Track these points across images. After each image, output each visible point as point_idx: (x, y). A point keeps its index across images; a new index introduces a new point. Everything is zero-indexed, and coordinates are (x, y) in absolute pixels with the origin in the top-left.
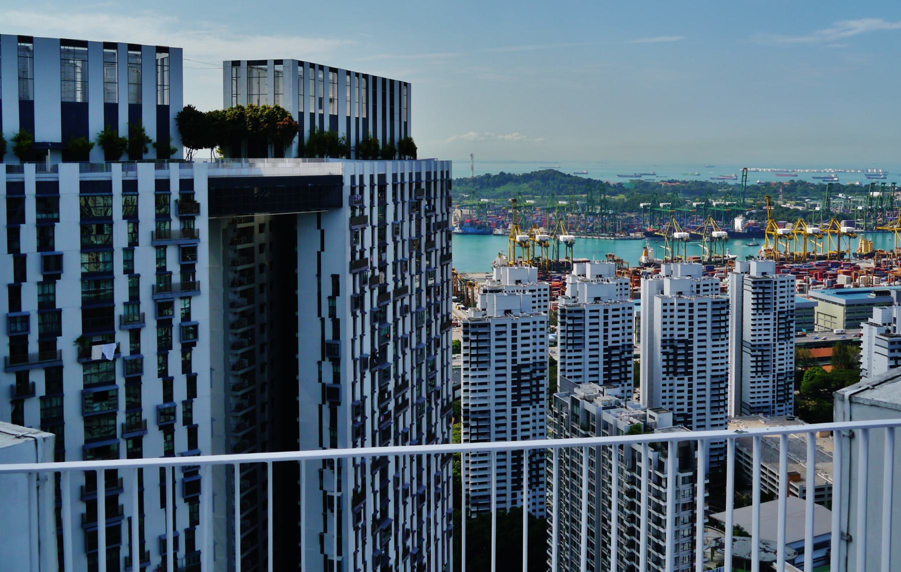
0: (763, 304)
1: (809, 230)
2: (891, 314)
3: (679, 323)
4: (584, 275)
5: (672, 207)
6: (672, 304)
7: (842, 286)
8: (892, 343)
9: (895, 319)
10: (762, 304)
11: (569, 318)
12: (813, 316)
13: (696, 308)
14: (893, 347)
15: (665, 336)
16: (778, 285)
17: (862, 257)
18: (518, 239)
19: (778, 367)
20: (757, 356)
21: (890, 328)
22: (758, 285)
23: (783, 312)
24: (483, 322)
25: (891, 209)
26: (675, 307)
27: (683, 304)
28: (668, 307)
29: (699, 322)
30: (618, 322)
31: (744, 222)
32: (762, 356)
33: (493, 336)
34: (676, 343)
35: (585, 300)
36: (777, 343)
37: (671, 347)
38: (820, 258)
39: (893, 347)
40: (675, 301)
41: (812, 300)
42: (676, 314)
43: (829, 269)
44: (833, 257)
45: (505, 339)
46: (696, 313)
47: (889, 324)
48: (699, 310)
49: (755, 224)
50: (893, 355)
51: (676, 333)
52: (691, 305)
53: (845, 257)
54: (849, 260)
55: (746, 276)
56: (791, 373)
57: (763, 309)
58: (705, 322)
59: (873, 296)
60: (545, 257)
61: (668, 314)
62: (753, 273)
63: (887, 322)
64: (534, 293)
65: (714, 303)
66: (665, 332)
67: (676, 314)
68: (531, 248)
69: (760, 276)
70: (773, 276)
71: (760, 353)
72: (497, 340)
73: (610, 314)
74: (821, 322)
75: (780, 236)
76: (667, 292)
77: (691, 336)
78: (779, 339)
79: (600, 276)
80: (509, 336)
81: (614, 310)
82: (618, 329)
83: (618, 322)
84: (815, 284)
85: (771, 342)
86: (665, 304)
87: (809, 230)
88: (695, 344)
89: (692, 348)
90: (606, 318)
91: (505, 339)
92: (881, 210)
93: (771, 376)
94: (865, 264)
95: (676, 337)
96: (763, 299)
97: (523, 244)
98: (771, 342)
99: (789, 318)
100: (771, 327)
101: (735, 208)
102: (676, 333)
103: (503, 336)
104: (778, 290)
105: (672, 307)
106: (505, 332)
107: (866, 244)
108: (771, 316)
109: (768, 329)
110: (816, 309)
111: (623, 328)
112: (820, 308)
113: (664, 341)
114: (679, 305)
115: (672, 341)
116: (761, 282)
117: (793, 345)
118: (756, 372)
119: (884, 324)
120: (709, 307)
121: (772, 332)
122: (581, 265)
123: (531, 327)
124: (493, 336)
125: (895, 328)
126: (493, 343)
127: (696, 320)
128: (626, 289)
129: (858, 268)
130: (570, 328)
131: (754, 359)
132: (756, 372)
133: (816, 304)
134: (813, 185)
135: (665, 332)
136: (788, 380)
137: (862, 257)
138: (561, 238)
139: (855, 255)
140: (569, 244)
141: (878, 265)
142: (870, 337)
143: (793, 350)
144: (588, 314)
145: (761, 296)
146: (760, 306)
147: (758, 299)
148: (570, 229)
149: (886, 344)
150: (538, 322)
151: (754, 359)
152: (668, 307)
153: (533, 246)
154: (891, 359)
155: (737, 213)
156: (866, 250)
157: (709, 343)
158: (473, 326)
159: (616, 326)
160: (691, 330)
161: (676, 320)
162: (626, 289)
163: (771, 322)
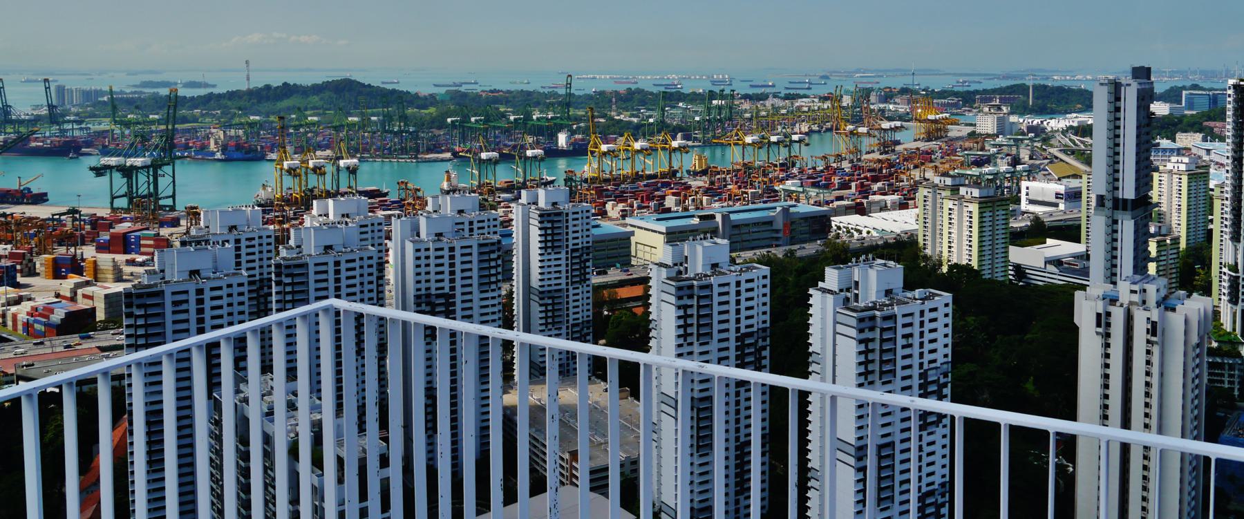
0: (553, 241)
1: (637, 145)
2: (683, 251)
3: (437, 273)
4: (327, 215)
5: (487, 121)
6: (428, 249)
7: (669, 210)
8: (679, 289)
10: (551, 242)
11: (287, 276)
12: (629, 247)
13: (457, 253)
15: (419, 290)
16: (571, 217)
17: (695, 174)
18: (286, 167)
19: (572, 317)
20: (546, 305)
22: (546, 218)
23: (577, 250)
24: (154, 289)
25: (730, 119)
26: (432, 253)
27: (442, 249)
28: (423, 254)
29: (463, 271)
30: (354, 277)
31: (569, 137)
32: (553, 304)
33: (169, 308)
34: (433, 299)
35: (311, 248)
36: (570, 288)
37: (427, 304)
38: (650, 177)
39: (681, 293)
40: (431, 245)
41: (629, 229)
42: (432, 261)
43: (658, 190)
44: (664, 175)
45: (187, 311)
46: (458, 260)
48: (462, 255)
49: (583, 140)
50: (681, 302)
51: (433, 285)
52: (452, 249)
53: (679, 175)
54: (681, 178)
55: (533, 207)
56: (588, 322)
57: (553, 247)
58: (470, 270)
59: (696, 221)
60: (322, 187)
61: (423, 262)
62: (542, 203)
63: (678, 262)
64: (253, 243)
65: (481, 245)
66: (419, 286)
67: (432, 261)
68: (303, 178)
69: (550, 207)
70: (566, 207)
71: (550, 301)
72: (174, 312)
73: (343, 267)
74: (640, 254)
75: (604, 154)
76: (423, 235)
77: (453, 288)
78: (573, 283)
79: (348, 216)
80: (192, 307)
81: (348, 261)
82: (354, 286)
83: (354, 277)
84: (640, 208)
85: (563, 286)
86: (418, 250)
87: (604, 148)
88: (458, 299)
89: (454, 304)
90: (337, 272)
91: (187, 311)
92: (720, 121)
93: (564, 328)
94: (696, 183)
95: (433, 292)
96: (553, 234)
97: (292, 171)
98: (563, 286)
99: (585, 257)
100: (563, 268)
101: (558, 121)
102: (433, 285)
103: (184, 307)
104: (571, 223)
105: (427, 253)
106: (187, 301)
107: (700, 159)
108: (563, 255)
109: (560, 272)
110: (633, 240)
111: (362, 284)
112: (639, 237)
113: (417, 297)
114: (436, 250)
115: (428, 296)
116: (549, 215)
117: (590, 289)
118: (546, 324)
119: (675, 265)
120: (475, 251)
121: (564, 275)
122: (322, 202)
123: (223, 293)
124: (169, 308)
126: (169, 318)
127: (458, 268)
128: (380, 231)
129: (690, 187)
130: (288, 289)
131: (543, 308)
132: (546, 324)
133: (632, 233)
134: (652, 94)
135: (419, 286)
136: (585, 331)
137: (696, 174)
138: (342, 163)
139: (688, 172)
140: (352, 171)
141: (712, 183)
143: (590, 295)
144: (312, 269)
145: (549, 232)
146: (549, 244)
147: (545, 235)
148: (352, 153)
149: (673, 290)
150: (235, 286)
151: (543, 308)
152: (423, 254)
153: (306, 174)
154: (679, 308)
155: (560, 128)
156: (700, 166)
157: (476, 295)
158: (139, 296)
159: (352, 282)
160: (452, 281)
161: (432, 269)
162: (380, 231)
163: (563, 262)
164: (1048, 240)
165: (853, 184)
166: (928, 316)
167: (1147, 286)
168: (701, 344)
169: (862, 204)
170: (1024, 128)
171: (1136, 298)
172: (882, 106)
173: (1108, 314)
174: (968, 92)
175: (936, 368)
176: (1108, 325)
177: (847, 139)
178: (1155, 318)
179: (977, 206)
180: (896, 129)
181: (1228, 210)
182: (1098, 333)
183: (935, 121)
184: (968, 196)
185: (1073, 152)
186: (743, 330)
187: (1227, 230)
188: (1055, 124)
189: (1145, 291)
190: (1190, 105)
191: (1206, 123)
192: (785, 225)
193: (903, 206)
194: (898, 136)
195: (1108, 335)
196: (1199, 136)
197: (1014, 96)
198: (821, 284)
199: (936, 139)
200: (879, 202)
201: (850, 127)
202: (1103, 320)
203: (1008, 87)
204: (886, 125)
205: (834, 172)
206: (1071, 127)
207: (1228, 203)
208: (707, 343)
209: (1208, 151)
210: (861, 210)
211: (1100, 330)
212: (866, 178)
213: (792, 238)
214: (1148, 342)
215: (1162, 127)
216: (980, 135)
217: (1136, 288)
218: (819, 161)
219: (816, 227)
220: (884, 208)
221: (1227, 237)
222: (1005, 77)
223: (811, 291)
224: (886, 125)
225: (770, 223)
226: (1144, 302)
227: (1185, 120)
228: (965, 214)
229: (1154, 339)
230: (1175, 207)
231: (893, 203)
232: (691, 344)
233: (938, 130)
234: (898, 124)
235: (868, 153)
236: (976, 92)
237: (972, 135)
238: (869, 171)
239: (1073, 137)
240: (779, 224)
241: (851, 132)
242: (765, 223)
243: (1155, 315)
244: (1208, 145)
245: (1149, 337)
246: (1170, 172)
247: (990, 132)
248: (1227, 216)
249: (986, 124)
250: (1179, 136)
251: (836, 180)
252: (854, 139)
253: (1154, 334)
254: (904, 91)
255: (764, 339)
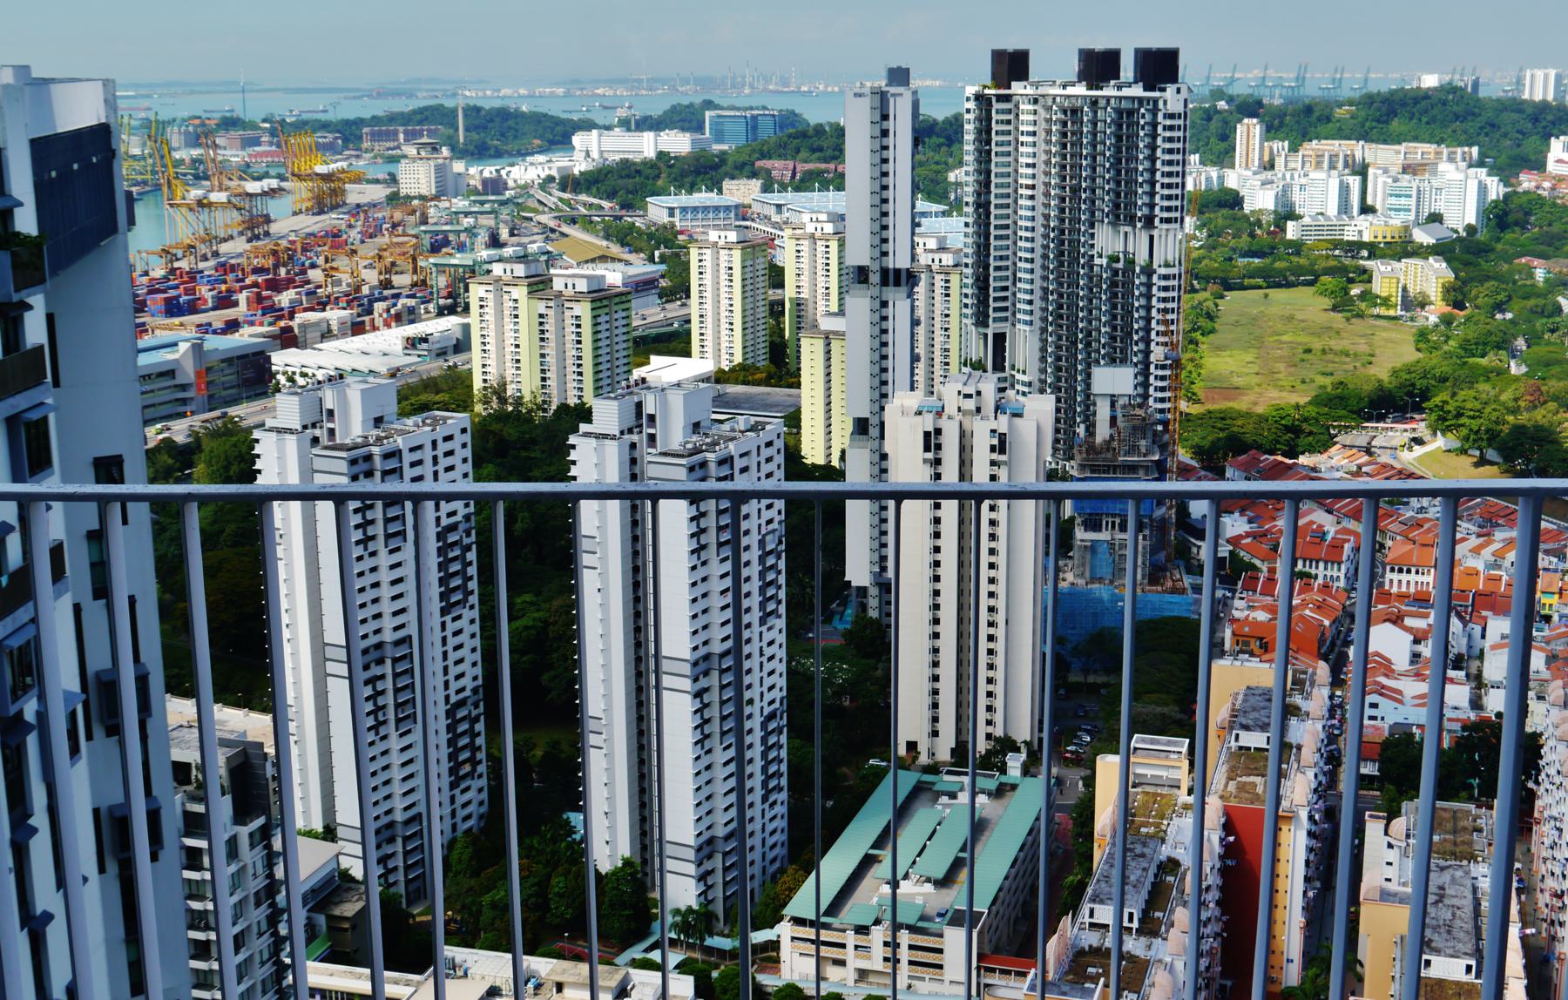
9: (331, 413)
14: (356, 469)
21: (317, 432)
39: (356, 469)
47: (314, 426)
119: (305, 427)
125: (332, 432)
142: (281, 458)
149: (343, 466)
164: (653, 358)
165: (242, 297)
166: (766, 453)
167: (981, 387)
168: (391, 552)
169: (290, 329)
170: (475, 182)
171: (970, 405)
172: (196, 152)
173: (938, 431)
174: (347, 123)
175: (774, 531)
176: (938, 447)
177: (191, 217)
178: (1003, 429)
179: (588, 306)
180: (272, 193)
181: (969, 281)
182: (925, 461)
183: (327, 178)
184: (569, 292)
185: (573, 221)
186: (445, 522)
187: (969, 311)
188: (526, 172)
189: (979, 393)
190: (719, 136)
191: (759, 164)
192: (198, 374)
193: (357, 329)
194: (274, 207)
195: (938, 462)
196: (756, 184)
197: (428, 122)
198: (583, 427)
199: (334, 207)
200: (317, 324)
201: (195, 193)
202: (932, 441)
203: (414, 112)
204: (253, 187)
205: (193, 275)
206: (551, 179)
207: (969, 271)
208: (398, 549)
209: (779, 206)
210: (288, 339)
211: (930, 455)
212: (255, 285)
213: (211, 397)
214: (993, 463)
215: (698, 173)
216: (409, 198)
217: (971, 390)
218: (154, 260)
219: (250, 374)
220: (327, 334)
221: (969, 321)
222: (381, 94)
223: (572, 440)
224: (253, 187)
225: (171, 373)
226: (978, 410)
227: (731, 160)
228: (569, 321)
229: (1003, 458)
230: (821, 291)
231: (342, 323)
232: (373, 554)
233: (334, 192)
234: (274, 183)
235: (225, 240)
236: (360, 122)
237: (394, 199)
238: (256, 271)
239: (566, 196)
240: (189, 372)
241: (200, 203)
242: (161, 375)
243: (1002, 424)
244: (776, 198)
245: (995, 456)
246: (812, 236)
247: (424, 192)
248: (969, 291)
249: (417, 177)
250: (727, 184)
251: (206, 293)
252: (204, 215)
253: (1002, 451)
254: (229, 123)
255: (468, 535)
